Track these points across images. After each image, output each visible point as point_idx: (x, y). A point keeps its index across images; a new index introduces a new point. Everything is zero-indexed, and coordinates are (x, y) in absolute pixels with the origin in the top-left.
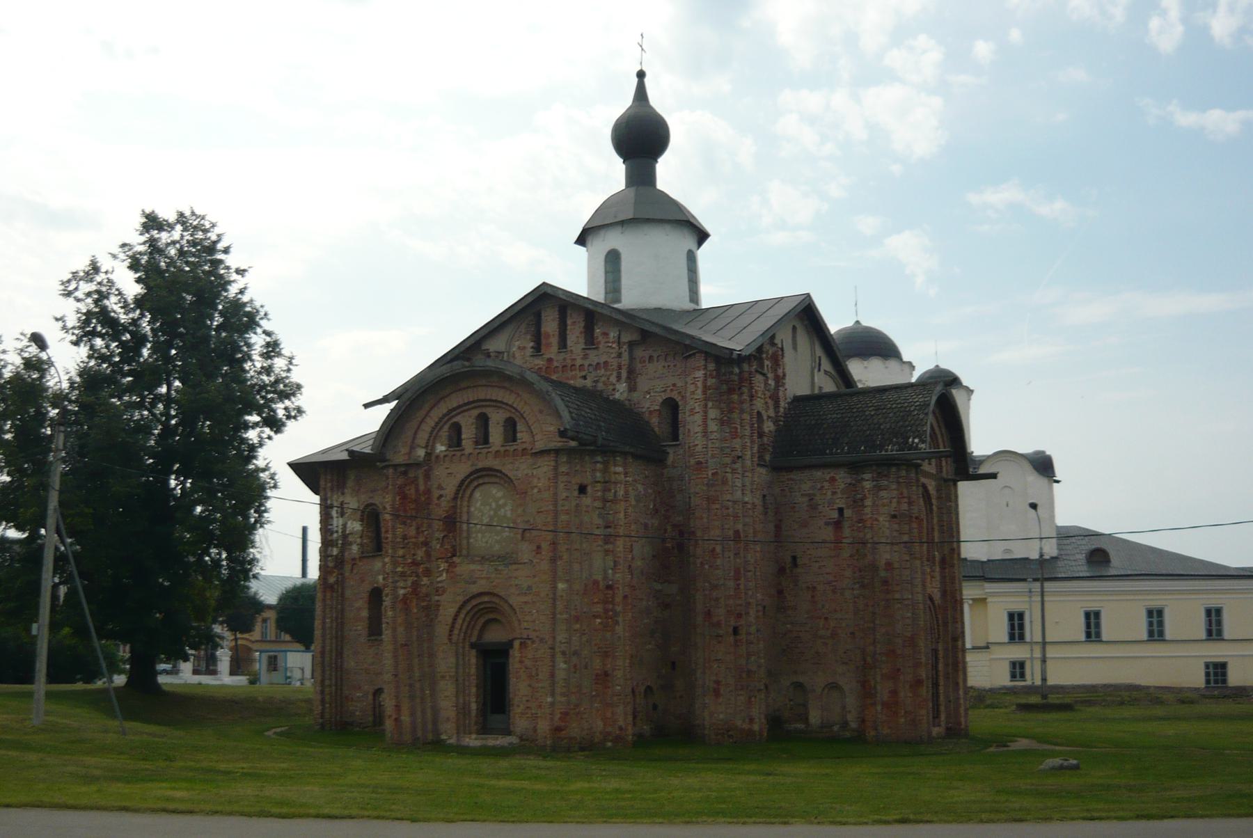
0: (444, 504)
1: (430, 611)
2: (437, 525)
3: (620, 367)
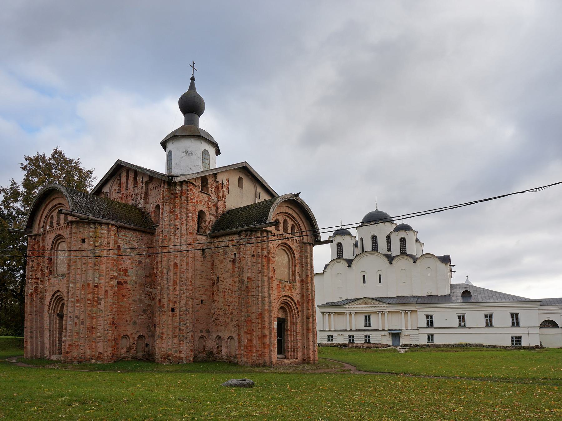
1: (42, 299)
3: (142, 194)
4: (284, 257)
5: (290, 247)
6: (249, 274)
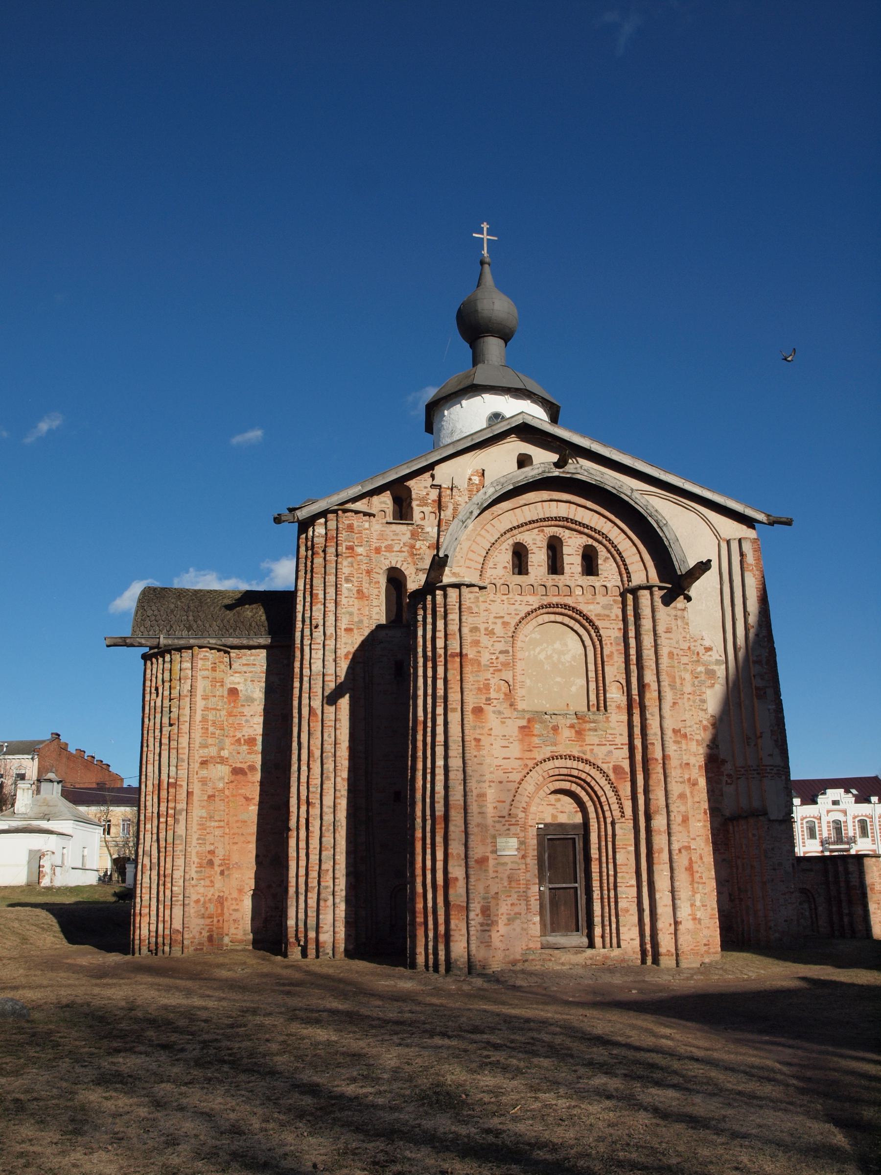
4: (566, 645)
5: (580, 613)
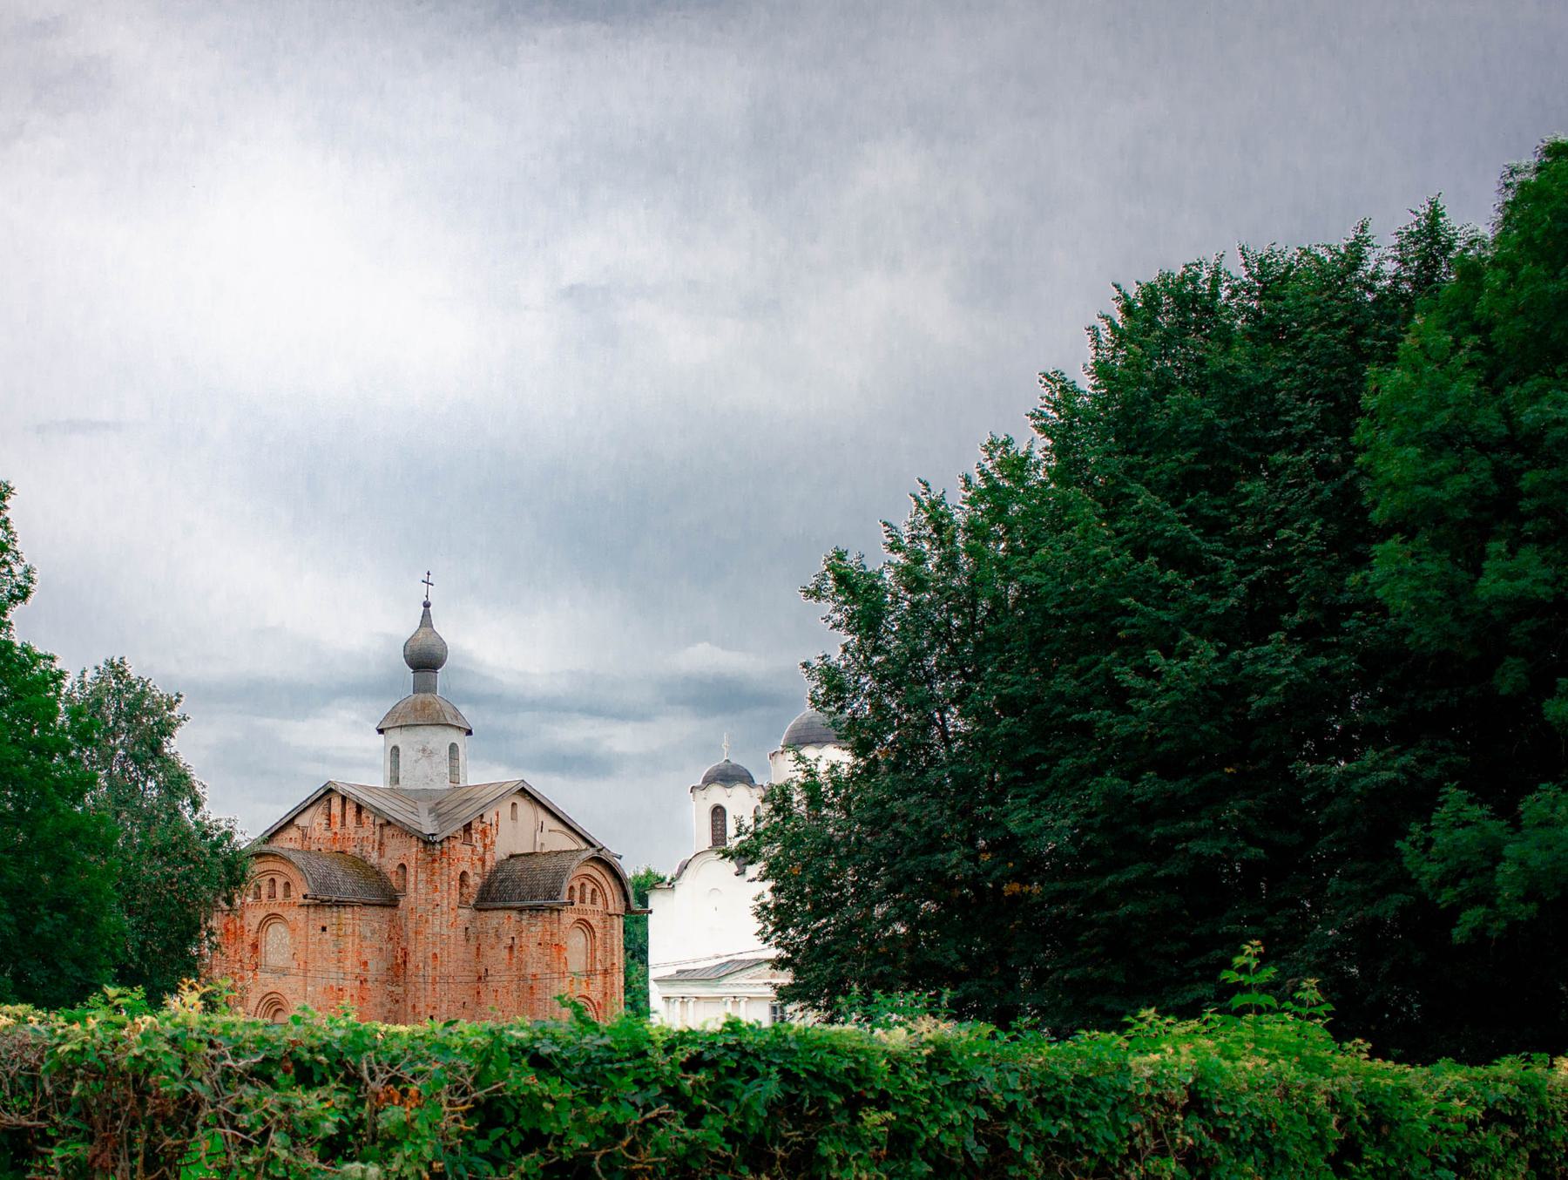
0: (252, 935)
2: (248, 948)
6: (534, 970)
